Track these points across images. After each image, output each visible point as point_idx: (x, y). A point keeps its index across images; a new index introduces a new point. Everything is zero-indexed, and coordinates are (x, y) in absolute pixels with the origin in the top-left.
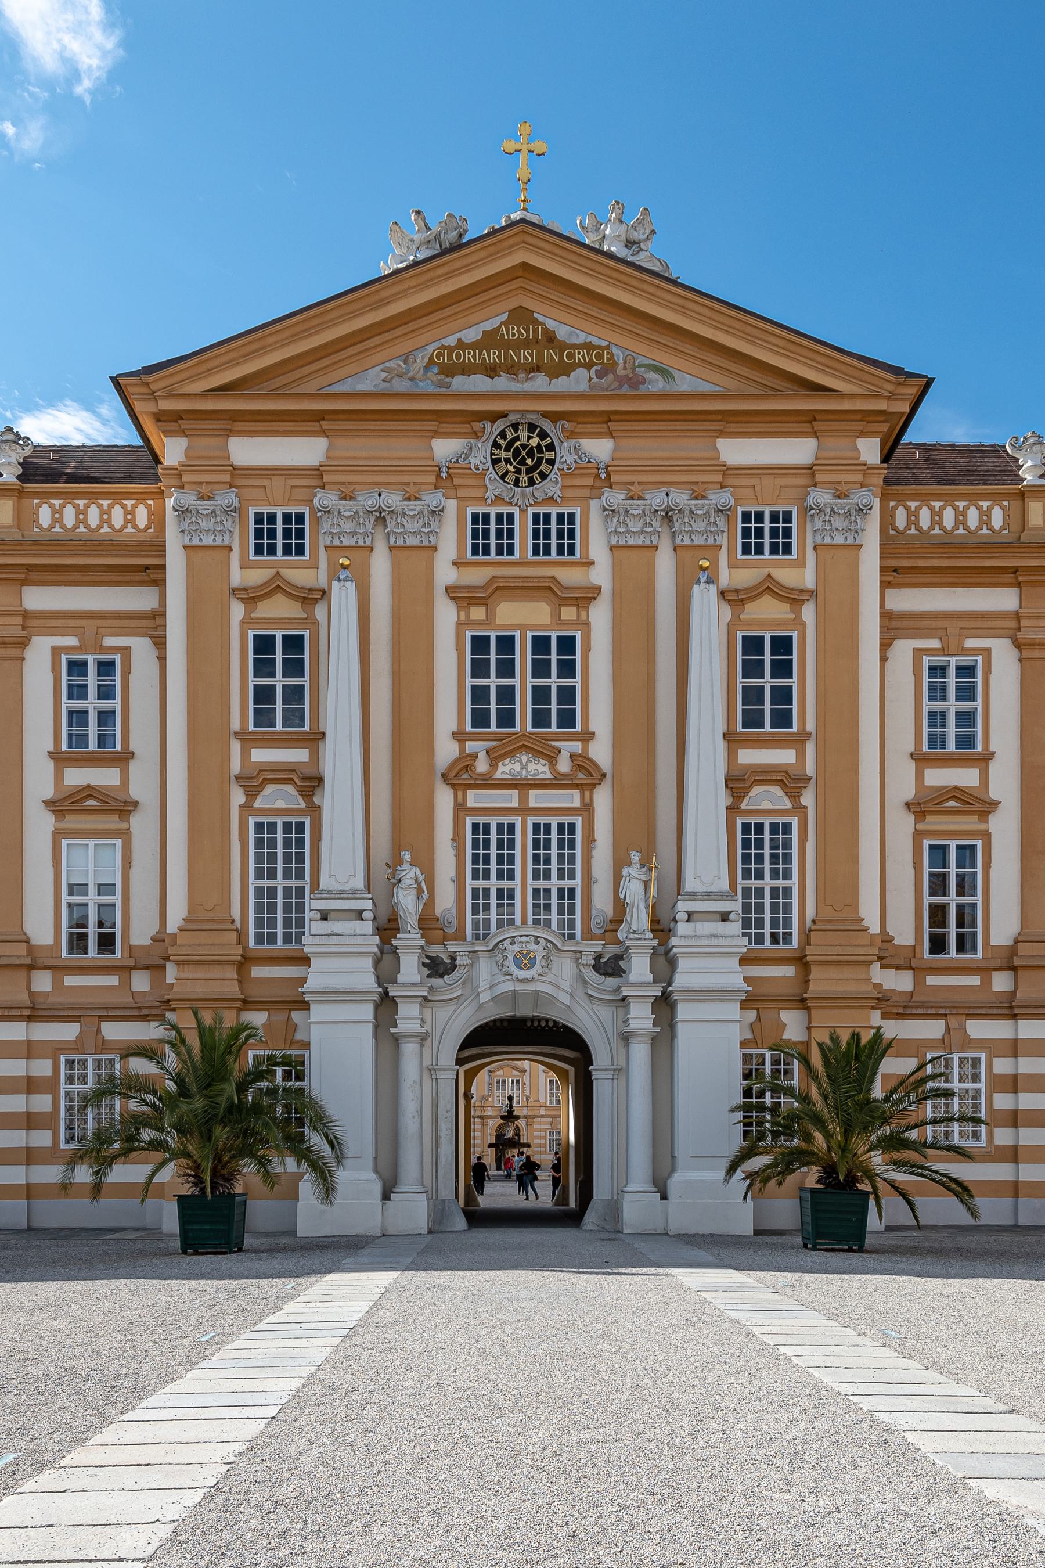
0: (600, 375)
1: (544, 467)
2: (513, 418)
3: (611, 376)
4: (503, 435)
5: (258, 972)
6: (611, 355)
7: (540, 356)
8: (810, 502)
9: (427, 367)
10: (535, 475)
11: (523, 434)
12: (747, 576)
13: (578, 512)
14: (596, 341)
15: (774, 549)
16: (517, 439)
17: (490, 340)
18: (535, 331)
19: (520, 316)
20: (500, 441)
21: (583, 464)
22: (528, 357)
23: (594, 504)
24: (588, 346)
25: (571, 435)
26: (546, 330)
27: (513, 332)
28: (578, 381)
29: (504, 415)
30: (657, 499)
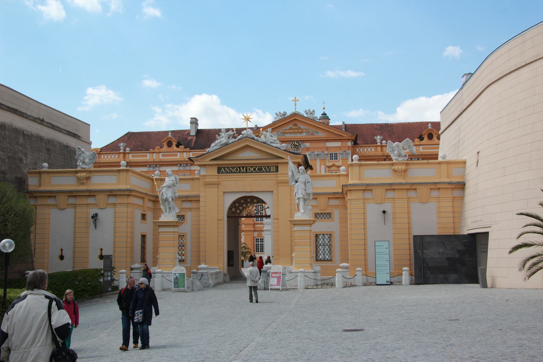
0: (307, 133)
1: (299, 148)
5: (256, 226)
6: (309, 130)
7: (298, 131)
11: (296, 143)
14: (307, 128)
15: (335, 159)
16: (295, 144)
17: (291, 129)
18: (297, 127)
21: (305, 147)
22: (296, 131)
24: (305, 129)
25: (303, 143)
26: (299, 127)
29: (293, 141)
30: (316, 153)
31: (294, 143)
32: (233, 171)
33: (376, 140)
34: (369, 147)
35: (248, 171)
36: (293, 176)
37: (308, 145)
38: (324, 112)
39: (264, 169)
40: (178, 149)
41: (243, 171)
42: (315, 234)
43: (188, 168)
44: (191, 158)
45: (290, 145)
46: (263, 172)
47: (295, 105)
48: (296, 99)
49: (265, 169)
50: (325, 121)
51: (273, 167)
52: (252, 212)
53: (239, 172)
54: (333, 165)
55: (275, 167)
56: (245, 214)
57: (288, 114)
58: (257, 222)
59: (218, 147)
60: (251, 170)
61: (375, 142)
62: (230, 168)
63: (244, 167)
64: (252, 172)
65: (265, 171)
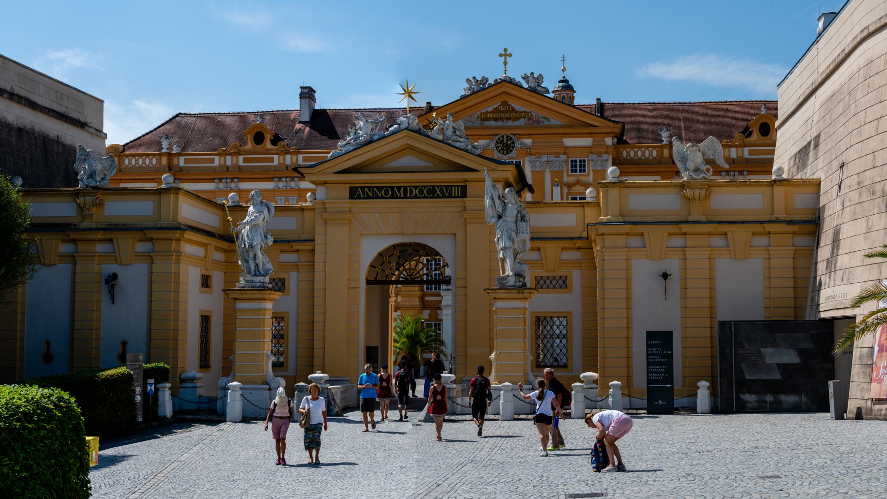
0: (528, 120)
2: (502, 134)
3: (531, 120)
4: (499, 139)
5: (427, 298)
6: (531, 114)
8: (589, 158)
9: (477, 118)
10: (509, 151)
11: (505, 139)
12: (572, 179)
13: (521, 160)
14: (527, 110)
15: (580, 171)
17: (495, 110)
19: (504, 103)
20: (498, 141)
22: (506, 115)
23: (527, 159)
24: (524, 112)
26: (512, 107)
27: (502, 108)
28: (522, 122)
31: (501, 139)
32: (380, 195)
33: (660, 136)
34: (647, 148)
35: (408, 195)
36: (493, 206)
37: (528, 141)
38: (564, 77)
39: (438, 191)
40: (274, 147)
41: (399, 195)
42: (536, 317)
43: (293, 184)
44: (298, 169)
45: (495, 142)
46: (438, 197)
47: (505, 63)
48: (508, 53)
49: (441, 191)
50: (565, 95)
51: (456, 188)
52: (416, 274)
53: (392, 197)
54: (578, 182)
55: (460, 188)
56: (402, 278)
57: (491, 81)
58: (429, 291)
59: (352, 148)
60: (414, 194)
61: (658, 138)
62: (373, 189)
63: (401, 187)
64: (416, 197)
65: (440, 195)
